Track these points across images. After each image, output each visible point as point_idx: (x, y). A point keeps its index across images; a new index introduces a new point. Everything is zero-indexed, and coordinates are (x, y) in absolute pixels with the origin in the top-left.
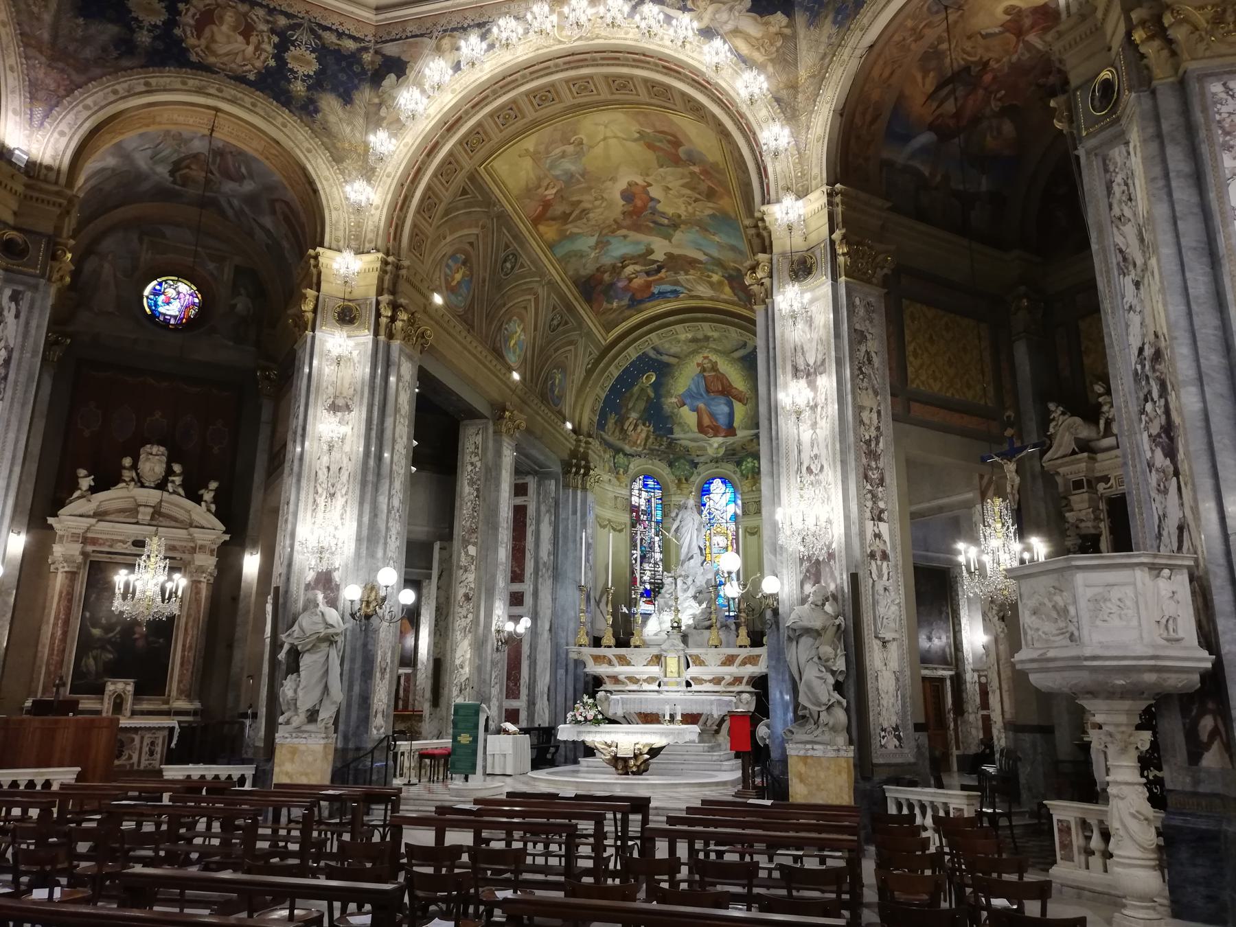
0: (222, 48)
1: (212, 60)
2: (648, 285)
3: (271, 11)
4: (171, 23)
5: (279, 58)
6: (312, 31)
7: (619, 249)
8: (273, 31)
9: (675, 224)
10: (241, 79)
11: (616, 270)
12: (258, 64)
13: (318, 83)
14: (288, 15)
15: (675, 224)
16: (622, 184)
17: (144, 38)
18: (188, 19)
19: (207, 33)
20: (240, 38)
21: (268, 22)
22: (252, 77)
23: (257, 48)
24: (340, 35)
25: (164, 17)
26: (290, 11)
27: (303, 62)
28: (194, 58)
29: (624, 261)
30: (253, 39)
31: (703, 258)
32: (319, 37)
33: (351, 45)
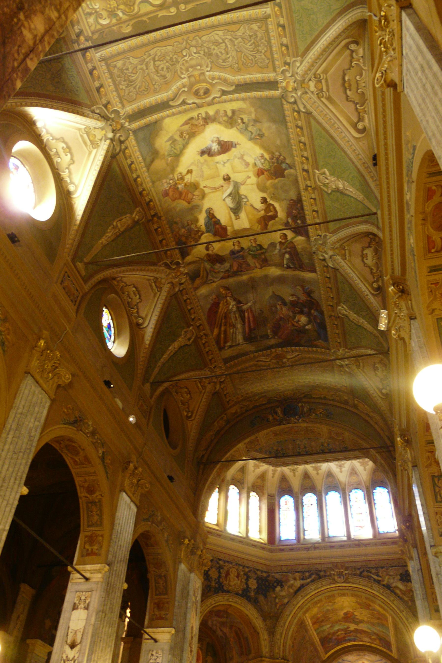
0: (232, 584)
1: (230, 588)
2: (344, 637)
3: (244, 567)
4: (219, 577)
5: (247, 584)
6: (254, 572)
7: (337, 627)
8: (244, 574)
9: (361, 622)
10: (237, 594)
11: (334, 634)
12: (241, 587)
13: (258, 590)
14: (248, 567)
15: (361, 622)
16: (345, 611)
17: (213, 584)
18: (223, 575)
19: (228, 579)
20: (236, 579)
21: (243, 571)
22: (240, 592)
23: (241, 582)
24: (262, 572)
25: (217, 576)
26: (248, 566)
27: (253, 584)
28: (225, 588)
29: (338, 630)
30: (240, 578)
31: (370, 631)
32: (256, 574)
33: (265, 575)
